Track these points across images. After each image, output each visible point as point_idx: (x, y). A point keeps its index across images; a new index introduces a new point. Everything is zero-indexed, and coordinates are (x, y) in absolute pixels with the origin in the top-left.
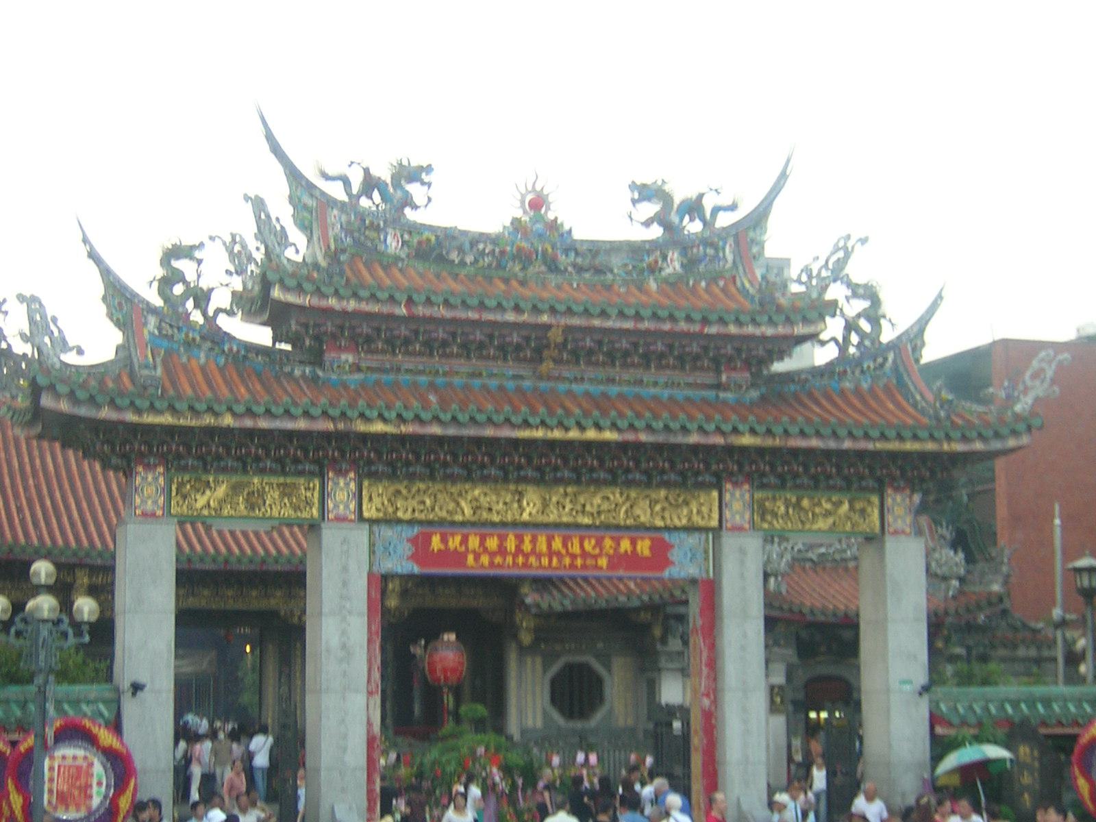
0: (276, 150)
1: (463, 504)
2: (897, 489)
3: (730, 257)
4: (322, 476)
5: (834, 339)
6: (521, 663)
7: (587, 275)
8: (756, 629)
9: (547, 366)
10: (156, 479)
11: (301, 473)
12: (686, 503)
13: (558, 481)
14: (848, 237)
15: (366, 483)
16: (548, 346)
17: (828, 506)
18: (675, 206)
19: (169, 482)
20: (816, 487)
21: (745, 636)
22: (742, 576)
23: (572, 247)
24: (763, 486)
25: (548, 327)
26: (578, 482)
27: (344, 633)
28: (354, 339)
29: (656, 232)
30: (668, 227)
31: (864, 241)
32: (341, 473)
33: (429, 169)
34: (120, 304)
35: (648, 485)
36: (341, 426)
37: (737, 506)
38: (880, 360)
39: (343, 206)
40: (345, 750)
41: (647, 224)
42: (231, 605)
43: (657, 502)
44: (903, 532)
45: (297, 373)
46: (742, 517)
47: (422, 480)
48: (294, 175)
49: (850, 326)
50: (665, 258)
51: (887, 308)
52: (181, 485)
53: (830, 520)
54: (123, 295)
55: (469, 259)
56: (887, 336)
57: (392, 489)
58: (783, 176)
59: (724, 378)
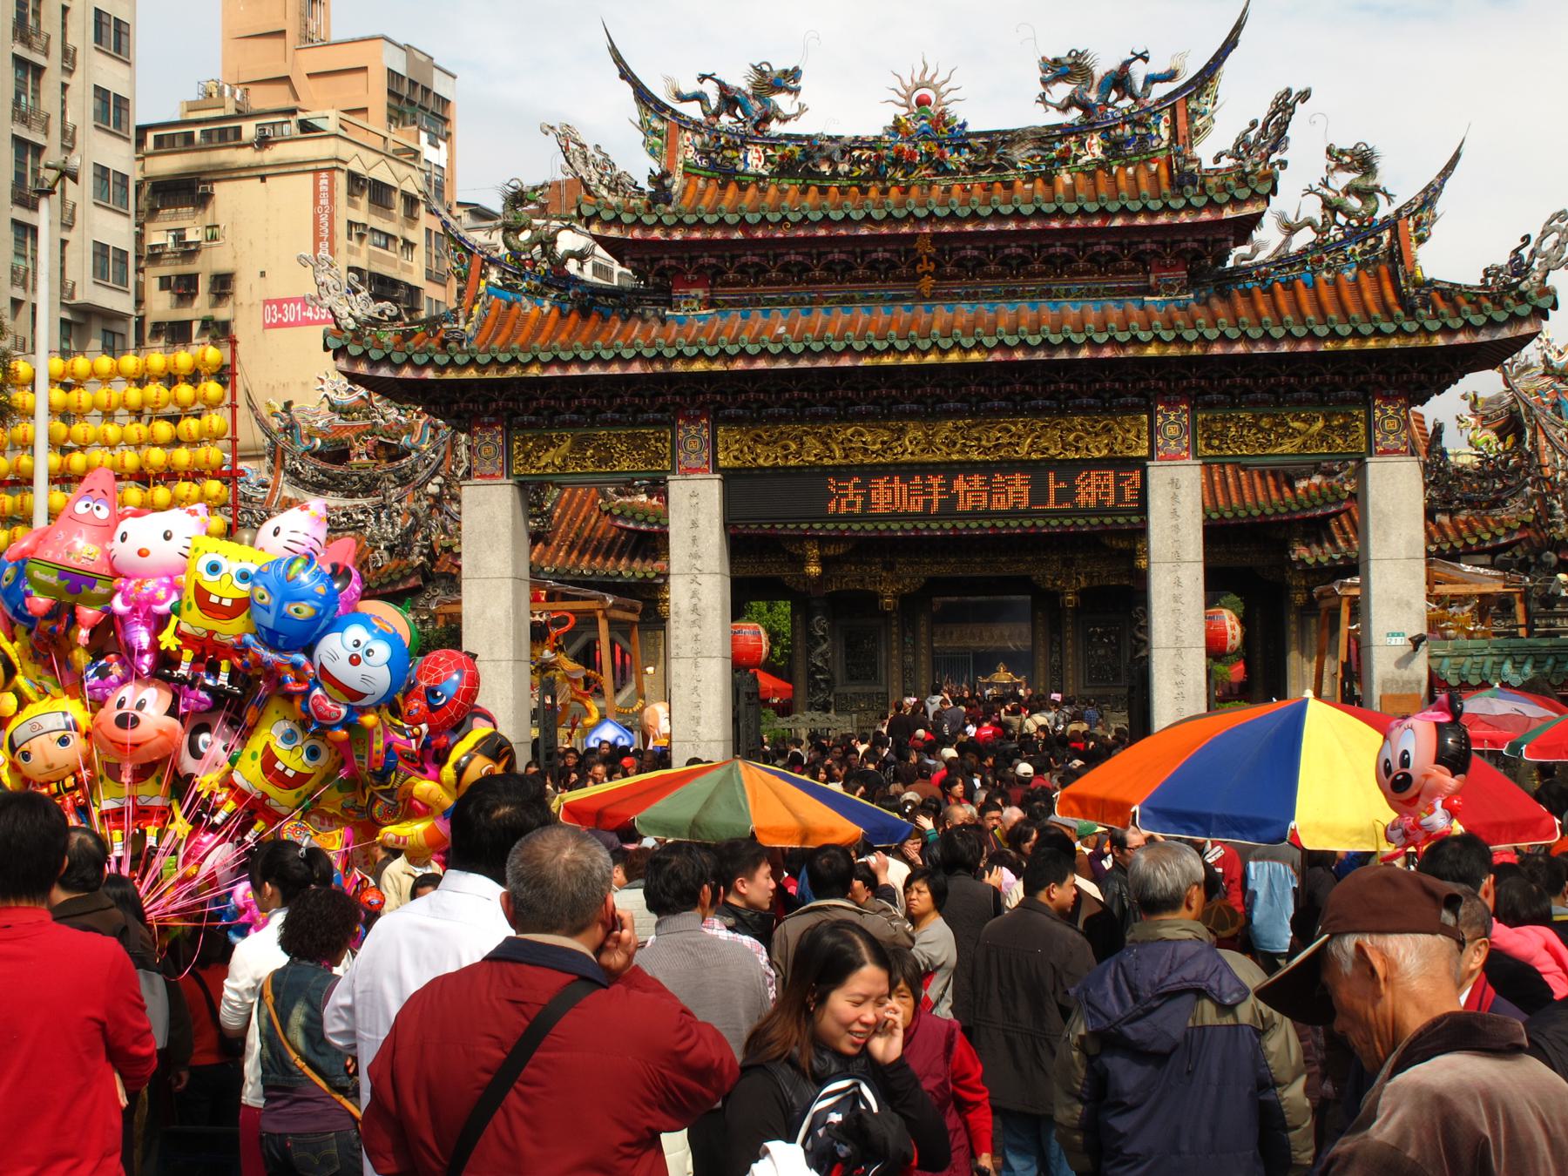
0: (626, 74)
1: (834, 446)
2: (1388, 400)
3: (1165, 134)
4: (672, 424)
5: (1310, 223)
6: (1303, 627)
7: (984, 174)
8: (1192, 576)
9: (927, 283)
10: (494, 437)
11: (646, 424)
12: (1107, 430)
13: (949, 415)
14: (1288, 92)
15: (721, 431)
16: (920, 260)
17: (1296, 425)
18: (1096, 81)
19: (508, 442)
20: (1279, 405)
21: (1178, 583)
22: (1174, 513)
23: (961, 139)
24: (1209, 406)
25: (912, 237)
26: (973, 415)
27: (694, 594)
28: (700, 270)
29: (1075, 114)
30: (1086, 107)
31: (1305, 96)
32: (694, 420)
33: (795, 74)
34: (460, 257)
35: (1062, 413)
36: (659, 367)
37: (1172, 430)
38: (1371, 241)
39: (696, 127)
40: (697, 721)
41: (1064, 108)
42: (978, 572)
43: (1070, 431)
44: (1397, 451)
45: (649, 314)
46: (1179, 443)
47: (788, 422)
48: (643, 95)
49: (1330, 207)
50: (1082, 144)
51: (1383, 178)
52: (524, 441)
53: (1299, 441)
54: (464, 248)
55: (844, 167)
56: (1384, 210)
57: (752, 434)
58: (1238, 28)
59: (1152, 279)
